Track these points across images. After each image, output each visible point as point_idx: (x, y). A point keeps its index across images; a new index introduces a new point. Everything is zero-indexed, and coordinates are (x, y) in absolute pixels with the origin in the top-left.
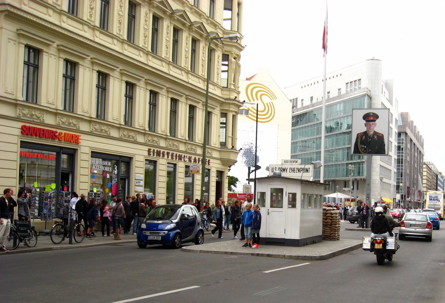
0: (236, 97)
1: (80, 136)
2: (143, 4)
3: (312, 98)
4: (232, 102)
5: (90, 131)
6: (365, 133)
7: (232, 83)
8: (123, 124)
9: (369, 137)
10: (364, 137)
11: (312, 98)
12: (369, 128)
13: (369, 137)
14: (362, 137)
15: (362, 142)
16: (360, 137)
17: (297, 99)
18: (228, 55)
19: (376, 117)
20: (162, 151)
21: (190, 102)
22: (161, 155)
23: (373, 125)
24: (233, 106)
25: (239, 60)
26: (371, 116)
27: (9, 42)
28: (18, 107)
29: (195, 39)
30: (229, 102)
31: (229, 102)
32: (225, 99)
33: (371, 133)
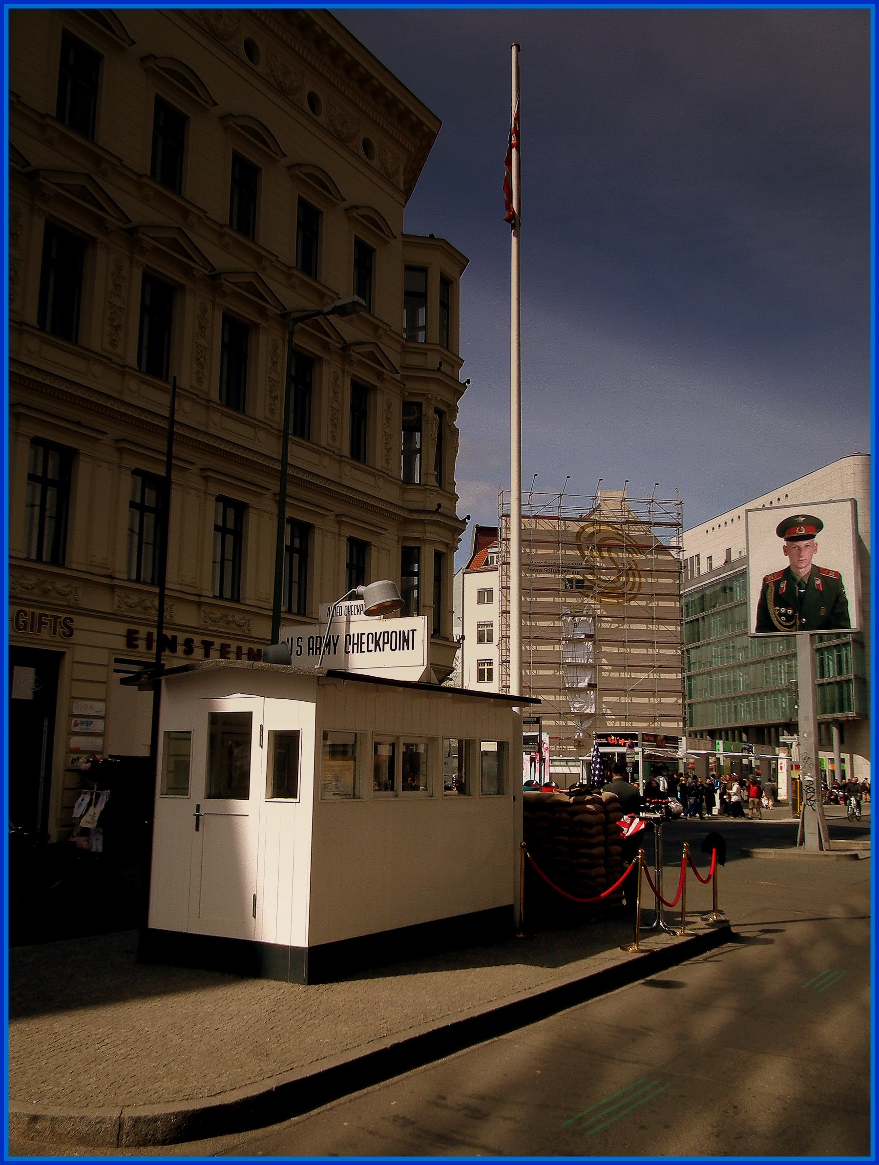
0: (439, 506)
2: (264, 324)
3: (728, 551)
6: (787, 573)
7: (432, 470)
9: (799, 585)
10: (783, 585)
11: (728, 551)
12: (796, 558)
13: (799, 585)
14: (777, 584)
15: (780, 600)
16: (772, 588)
17: (698, 556)
18: (420, 405)
19: (816, 525)
20: (181, 638)
21: (348, 532)
22: (180, 649)
23: (809, 549)
24: (435, 529)
32: (411, 511)
33: (804, 572)
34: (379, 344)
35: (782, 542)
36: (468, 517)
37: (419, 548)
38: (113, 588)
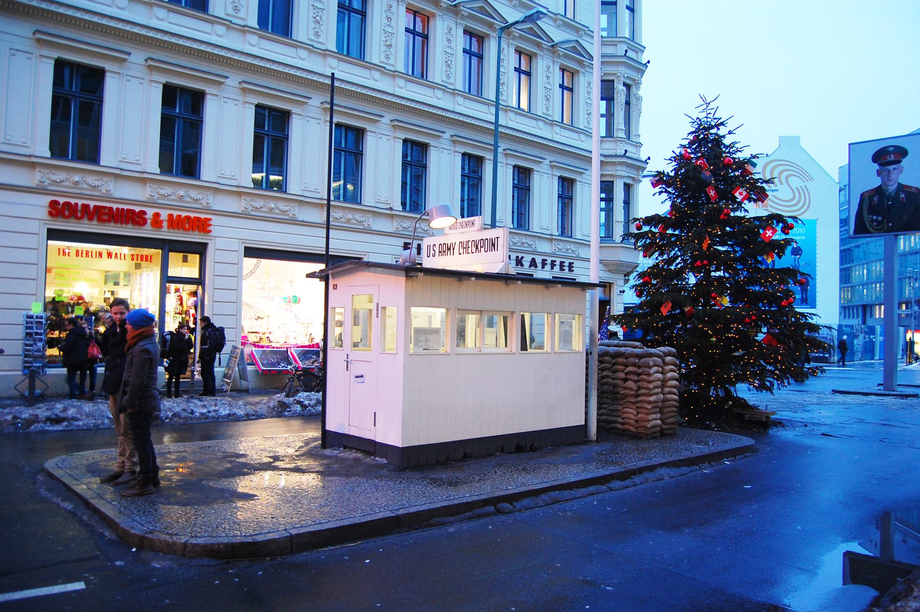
0: (626, 151)
1: (210, 219)
4: (618, 160)
5: (240, 211)
6: (879, 190)
8: (400, 208)
10: (875, 199)
12: (886, 179)
15: (873, 210)
16: (867, 200)
18: (613, 81)
19: (901, 152)
23: (896, 172)
24: (624, 168)
25: (638, 89)
26: (890, 153)
27: (14, 55)
28: (148, 185)
29: (468, 29)
30: (614, 160)
31: (614, 160)
33: (892, 188)
34: (580, 41)
35: (876, 167)
36: (649, 158)
37: (612, 182)
38: (392, 216)
